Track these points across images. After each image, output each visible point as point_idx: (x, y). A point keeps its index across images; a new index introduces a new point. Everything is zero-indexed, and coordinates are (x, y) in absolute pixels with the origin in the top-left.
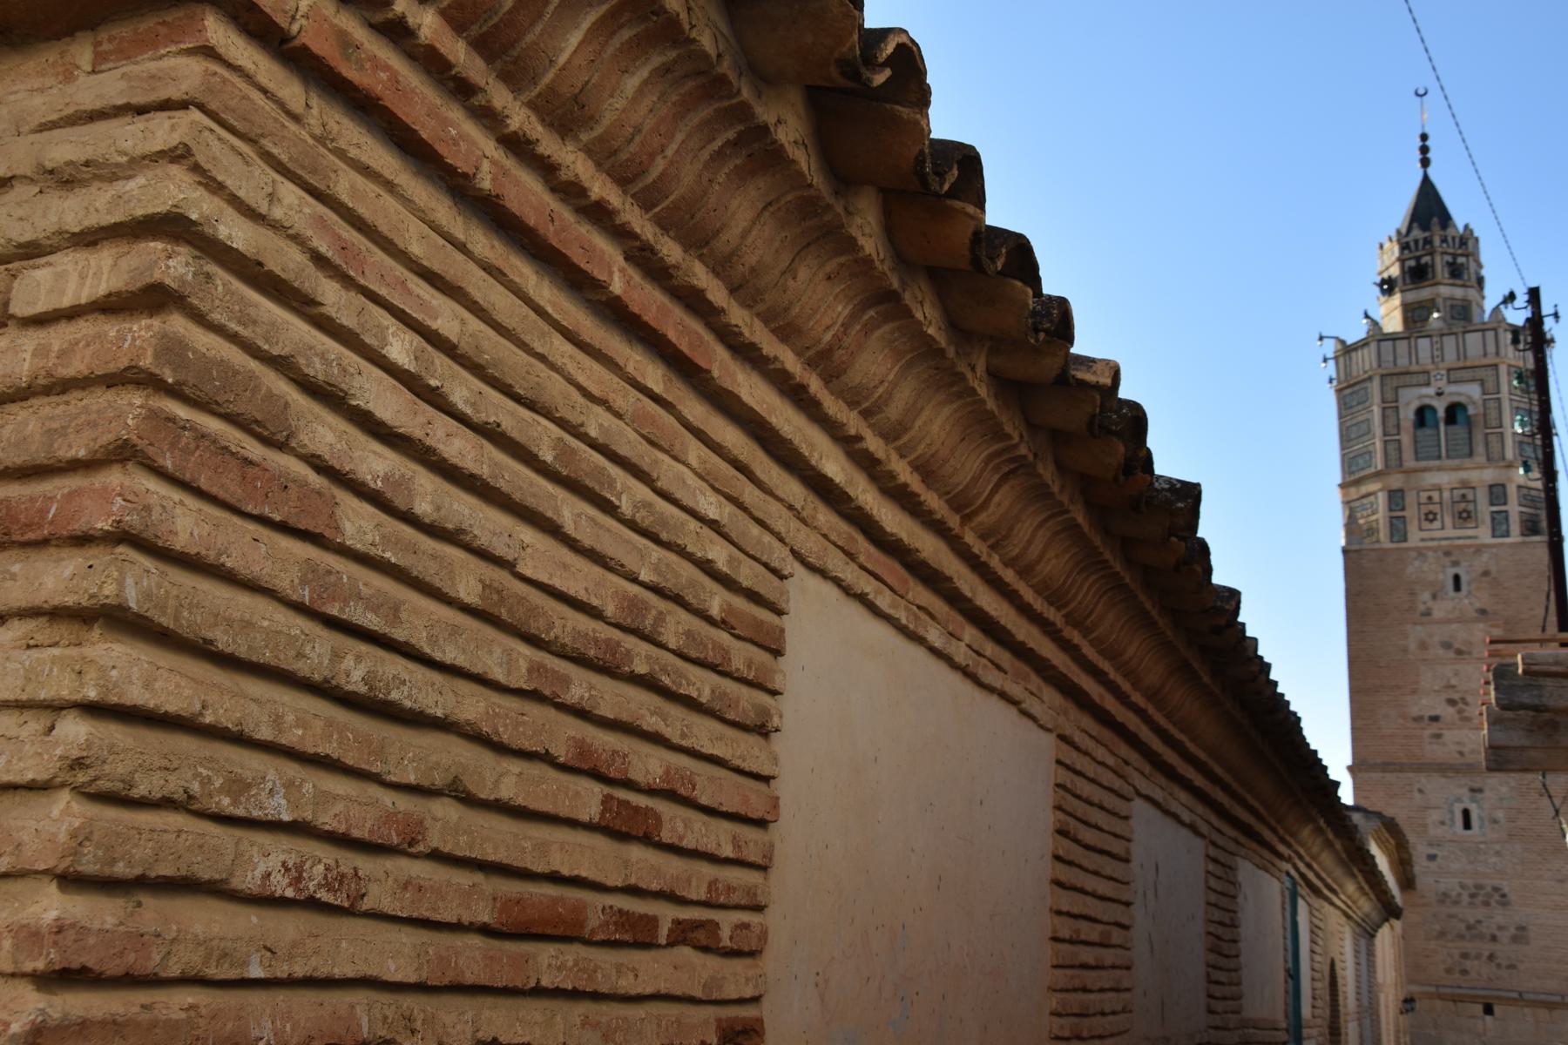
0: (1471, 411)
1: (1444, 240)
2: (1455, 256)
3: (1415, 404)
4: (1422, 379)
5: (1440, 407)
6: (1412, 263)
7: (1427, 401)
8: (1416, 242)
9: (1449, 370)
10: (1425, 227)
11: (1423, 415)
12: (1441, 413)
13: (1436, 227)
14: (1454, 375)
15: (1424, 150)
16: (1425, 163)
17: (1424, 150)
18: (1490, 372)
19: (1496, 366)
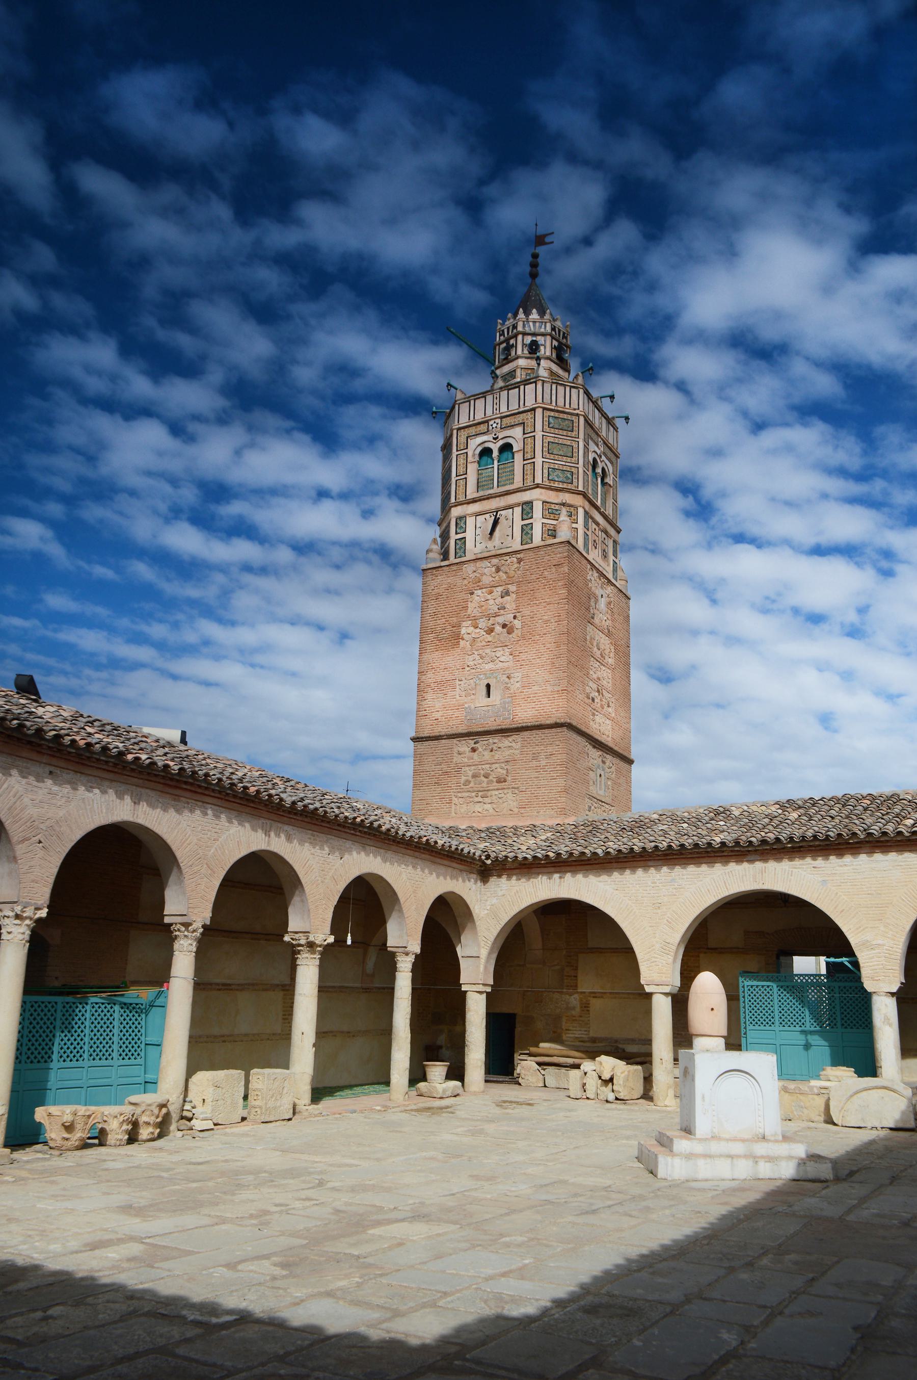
3: (480, 449)
4: (483, 428)
5: (495, 448)
7: (486, 445)
8: (508, 328)
12: (495, 454)
14: (506, 421)
17: (534, 265)
18: (530, 415)
19: (534, 410)
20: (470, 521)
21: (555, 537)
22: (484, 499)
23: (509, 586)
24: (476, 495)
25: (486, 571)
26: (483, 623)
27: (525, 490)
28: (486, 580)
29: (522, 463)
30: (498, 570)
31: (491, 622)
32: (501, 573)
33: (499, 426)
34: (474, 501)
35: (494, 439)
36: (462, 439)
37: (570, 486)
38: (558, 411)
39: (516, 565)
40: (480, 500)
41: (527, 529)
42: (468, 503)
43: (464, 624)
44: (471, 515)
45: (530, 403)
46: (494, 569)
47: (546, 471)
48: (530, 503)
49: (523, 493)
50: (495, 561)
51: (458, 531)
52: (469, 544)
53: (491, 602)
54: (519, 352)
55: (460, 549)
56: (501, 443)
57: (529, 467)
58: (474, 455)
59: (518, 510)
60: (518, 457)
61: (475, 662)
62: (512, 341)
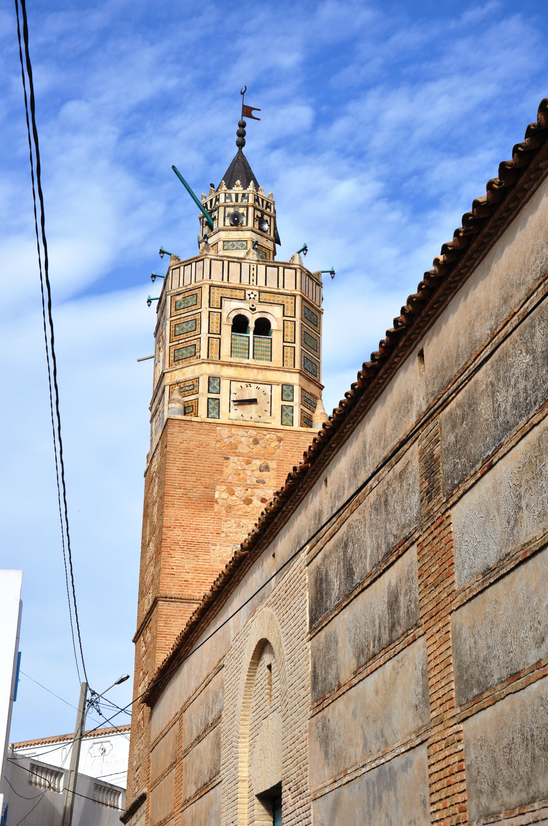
0: (274, 326)
1: (256, 200)
2: (263, 213)
4: (240, 294)
6: (231, 210)
7: (242, 312)
8: (237, 195)
9: (260, 292)
10: (245, 187)
11: (240, 324)
12: (252, 325)
13: (251, 187)
15: (241, 134)
16: (241, 144)
17: (241, 134)
18: (290, 300)
19: (295, 296)
20: (225, 384)
21: (312, 427)
22: (241, 367)
23: (269, 462)
24: (230, 360)
25: (243, 439)
26: (239, 491)
27: (285, 371)
28: (243, 449)
29: (281, 344)
30: (256, 442)
31: (249, 492)
32: (258, 446)
33: (257, 298)
34: (230, 365)
35: (251, 309)
36: (216, 297)
37: (315, 378)
38: (309, 304)
39: (276, 443)
40: (236, 366)
41: (288, 411)
42: (223, 365)
43: (218, 487)
44: (227, 378)
45: (290, 287)
46: (251, 440)
47: (303, 359)
48: (291, 386)
49: (283, 374)
50: (252, 432)
51: (211, 390)
52: (224, 407)
53: (249, 473)
54: (250, 224)
55: (214, 409)
56: (258, 316)
57: (289, 350)
58: (228, 317)
59: (277, 390)
60: (276, 337)
61: (232, 530)
62: (242, 210)
